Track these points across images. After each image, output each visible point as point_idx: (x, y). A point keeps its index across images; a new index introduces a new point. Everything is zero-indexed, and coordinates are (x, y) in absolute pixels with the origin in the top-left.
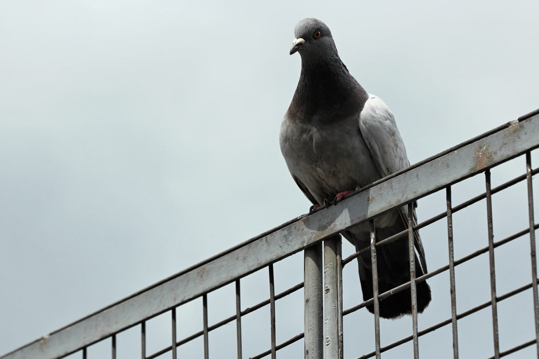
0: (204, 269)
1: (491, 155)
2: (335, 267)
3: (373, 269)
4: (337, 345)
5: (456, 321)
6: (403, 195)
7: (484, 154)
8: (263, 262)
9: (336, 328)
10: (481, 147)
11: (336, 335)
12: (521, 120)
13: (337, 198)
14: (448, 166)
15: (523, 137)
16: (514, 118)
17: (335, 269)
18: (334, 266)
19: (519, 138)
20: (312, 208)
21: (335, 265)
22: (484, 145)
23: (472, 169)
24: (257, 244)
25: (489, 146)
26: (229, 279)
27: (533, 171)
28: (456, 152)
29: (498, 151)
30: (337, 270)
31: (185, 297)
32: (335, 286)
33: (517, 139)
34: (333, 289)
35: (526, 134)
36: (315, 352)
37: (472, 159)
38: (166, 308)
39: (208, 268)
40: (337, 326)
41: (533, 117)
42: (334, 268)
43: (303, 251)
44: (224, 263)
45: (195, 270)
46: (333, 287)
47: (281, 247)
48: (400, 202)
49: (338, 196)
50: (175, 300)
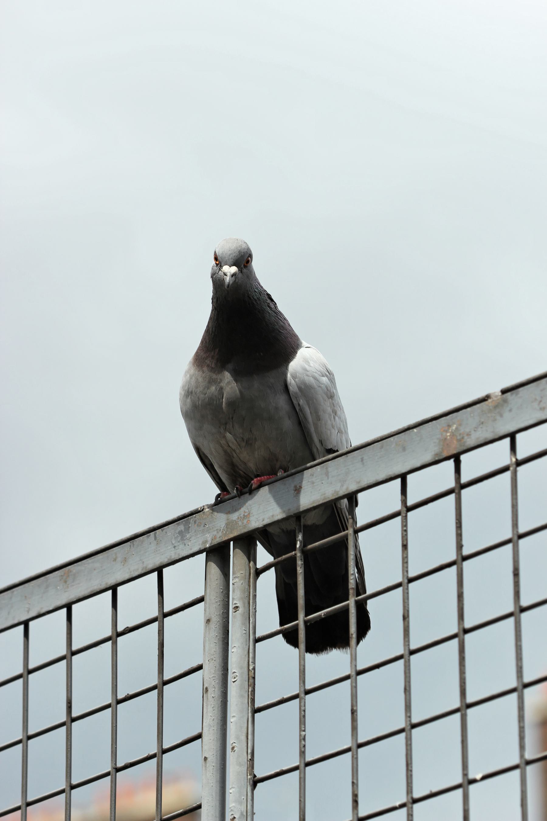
0: (70, 571)
1: (463, 438)
2: (247, 577)
3: (298, 583)
4: (247, 683)
5: (409, 657)
6: (342, 486)
7: (453, 435)
8: (150, 566)
9: (247, 659)
10: (449, 426)
11: (246, 669)
12: (504, 392)
13: (252, 485)
14: (404, 449)
15: (507, 415)
16: (495, 389)
17: (247, 580)
18: (245, 575)
19: (501, 416)
20: (218, 496)
21: (247, 574)
22: (454, 423)
23: (436, 455)
24: (142, 542)
25: (460, 425)
26: (103, 587)
27: (518, 462)
28: (415, 430)
29: (473, 432)
30: (249, 582)
31: (42, 608)
32: (247, 605)
33: (498, 417)
34: (244, 606)
35: (510, 410)
36: (216, 690)
37: (437, 441)
38: (16, 621)
39: (74, 571)
40: (247, 656)
41: (521, 389)
42: (246, 578)
43: (205, 554)
44: (97, 565)
45: (57, 572)
46: (244, 603)
47: (175, 547)
48: (338, 494)
49: (254, 482)
50: (28, 612)
